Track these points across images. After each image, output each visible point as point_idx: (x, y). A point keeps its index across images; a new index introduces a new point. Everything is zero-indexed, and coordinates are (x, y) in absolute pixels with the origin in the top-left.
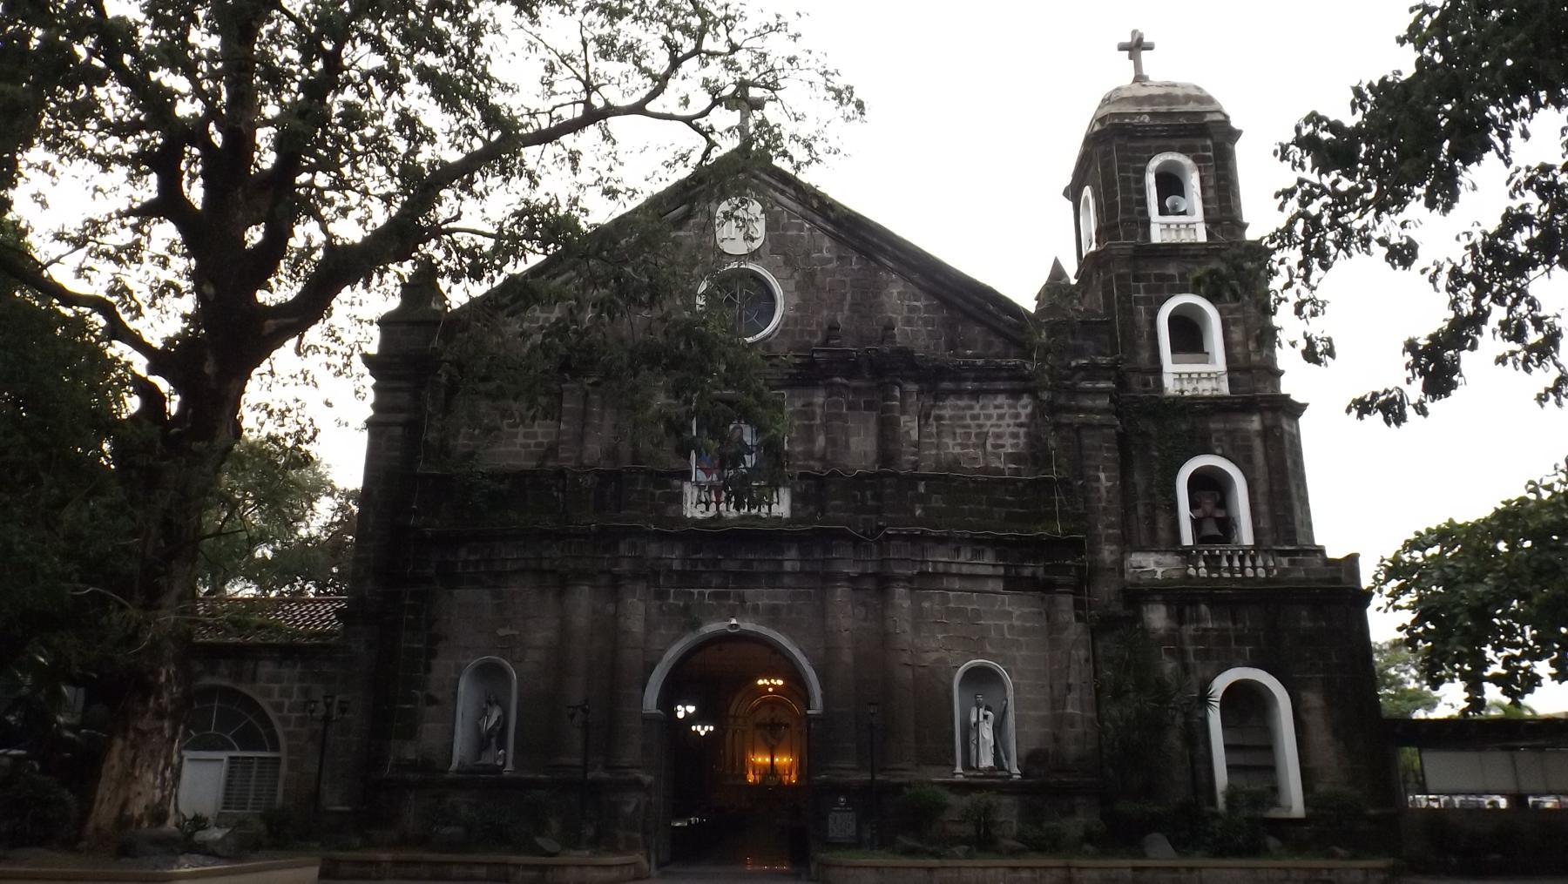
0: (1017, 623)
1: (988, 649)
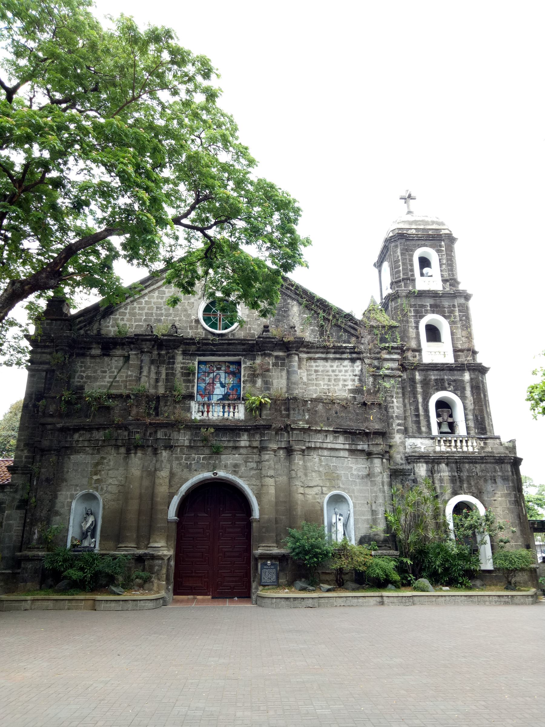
0: (355, 473)
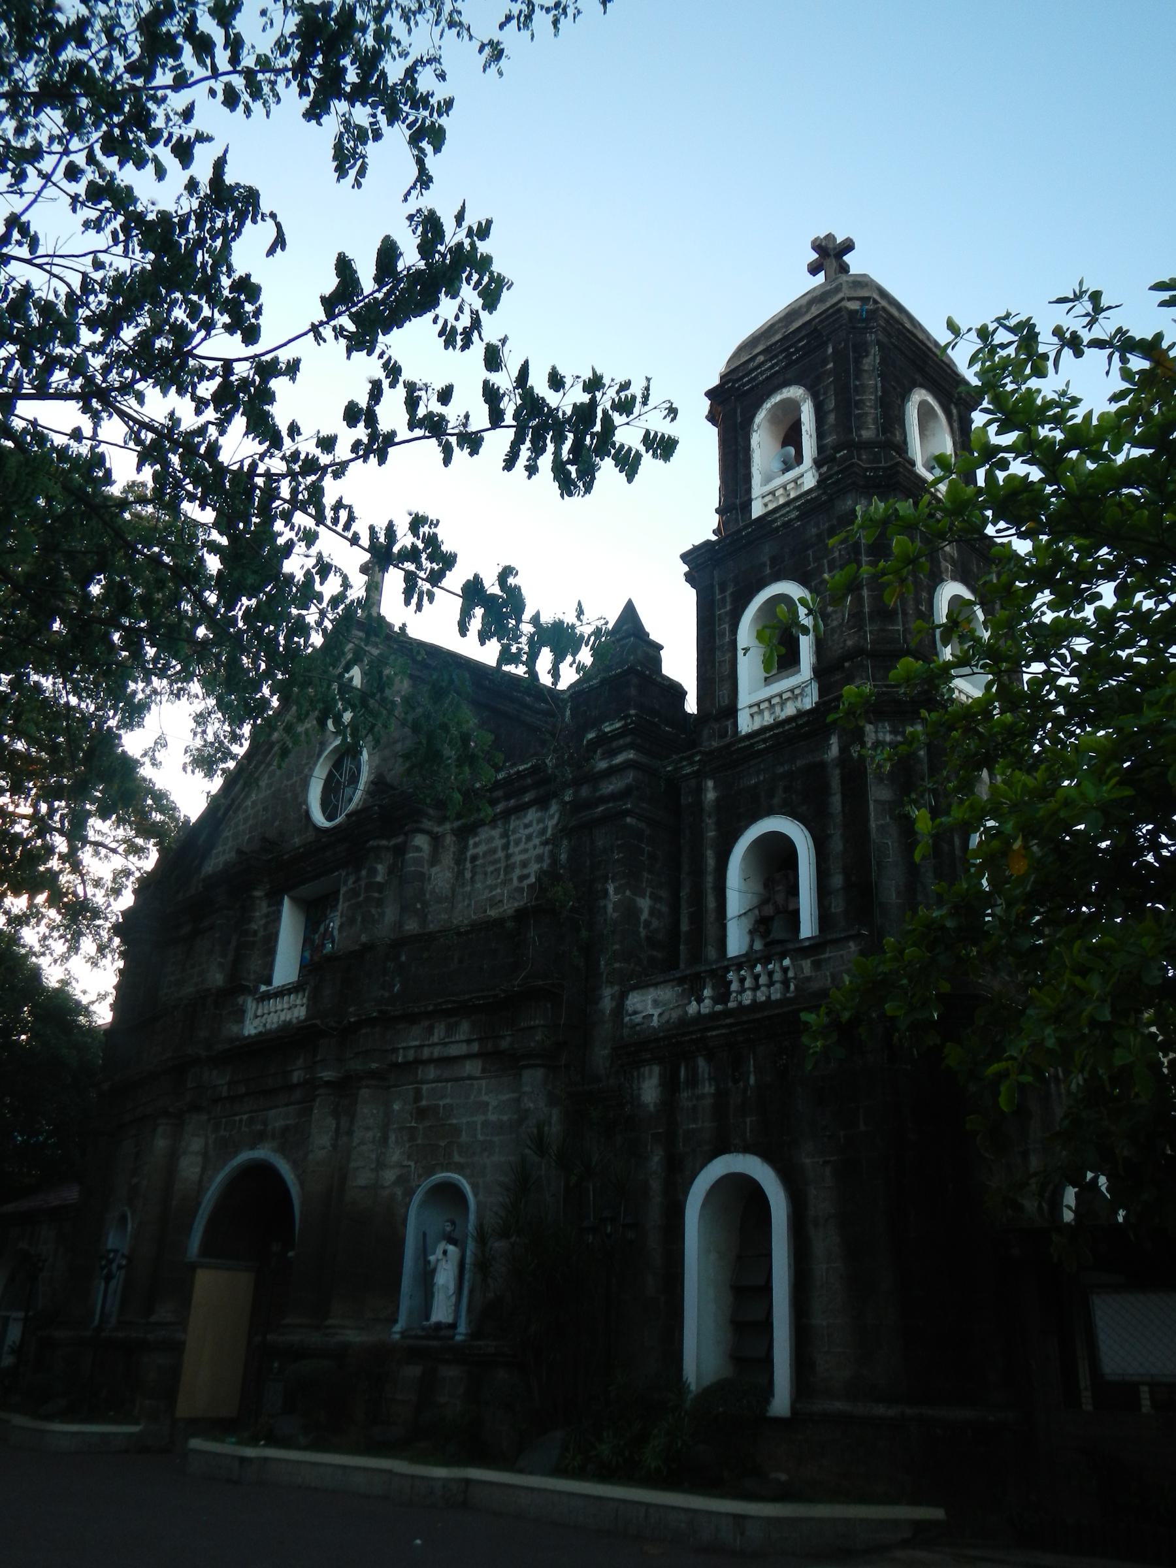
0: (492, 1117)
1: (457, 1158)
